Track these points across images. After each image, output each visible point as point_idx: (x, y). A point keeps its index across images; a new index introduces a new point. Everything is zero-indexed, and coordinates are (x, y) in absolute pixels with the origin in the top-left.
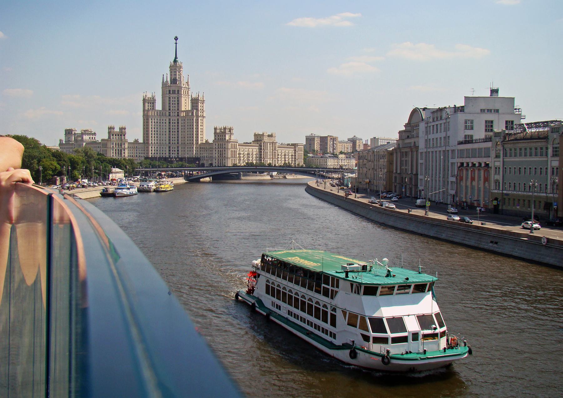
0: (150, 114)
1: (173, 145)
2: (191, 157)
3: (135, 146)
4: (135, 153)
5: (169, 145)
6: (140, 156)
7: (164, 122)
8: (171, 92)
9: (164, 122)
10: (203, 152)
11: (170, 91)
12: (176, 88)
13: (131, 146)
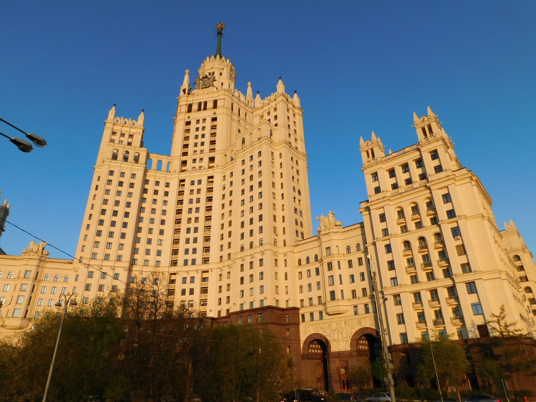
1: (186, 268)
2: (257, 305)
3: (23, 269)
5: (173, 269)
8: (195, 107)
9: (161, 189)
10: (314, 279)
11: (190, 106)
12: (210, 96)
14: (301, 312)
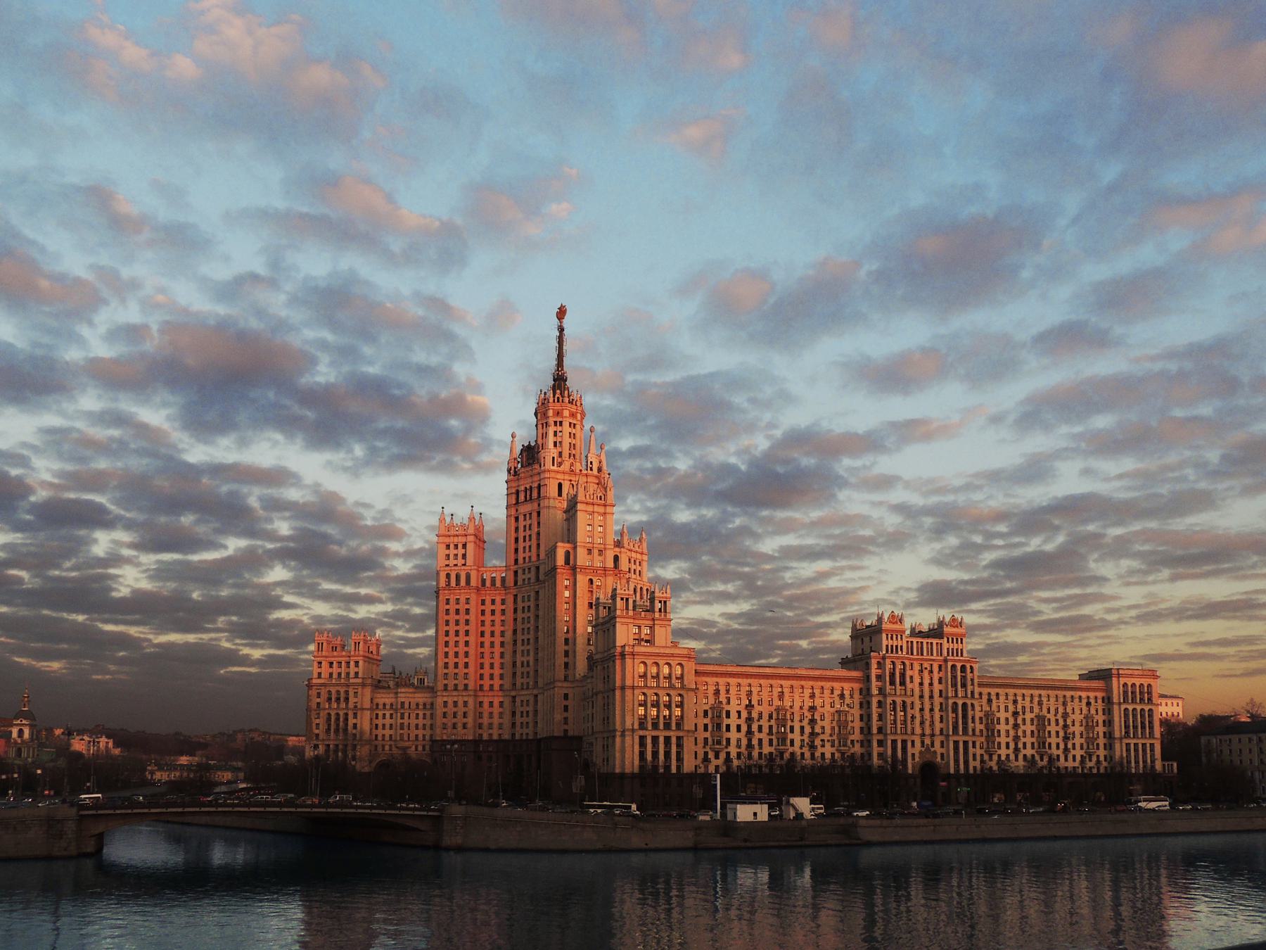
0: (443, 583)
1: (523, 692)
4: (398, 724)
5: (513, 693)
6: (417, 736)
7: (498, 607)
13: (388, 701)
14: (584, 738)
